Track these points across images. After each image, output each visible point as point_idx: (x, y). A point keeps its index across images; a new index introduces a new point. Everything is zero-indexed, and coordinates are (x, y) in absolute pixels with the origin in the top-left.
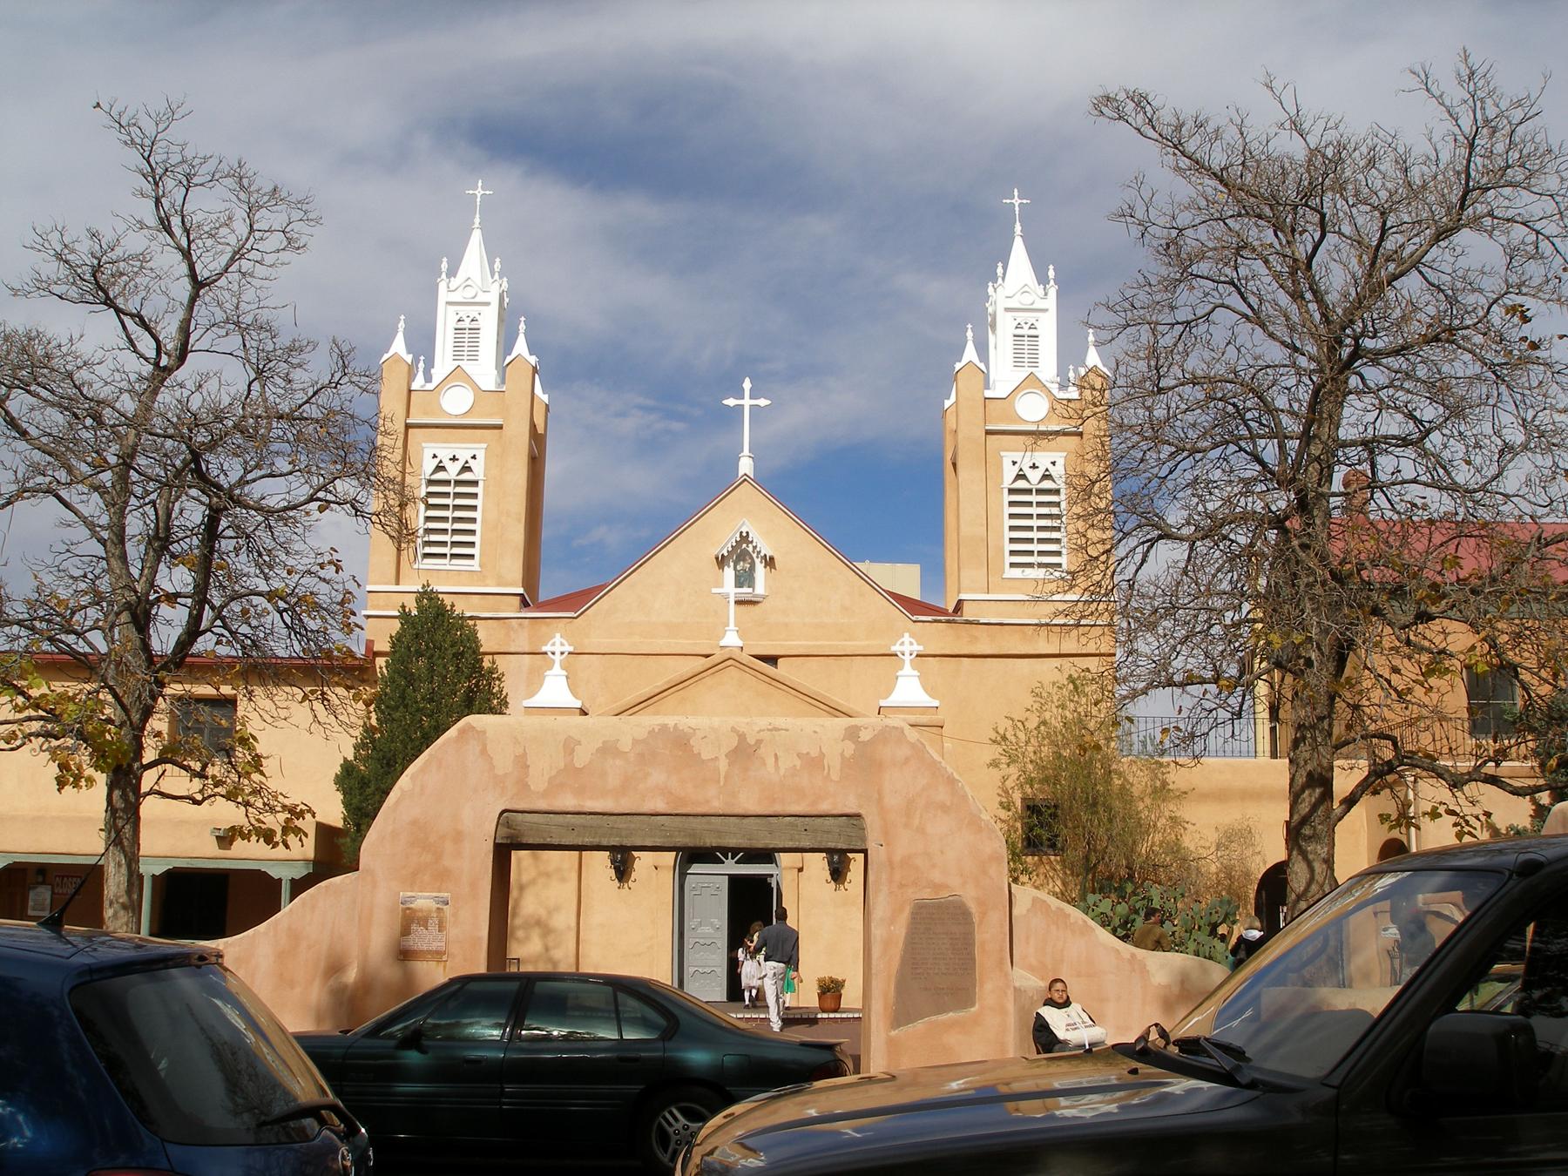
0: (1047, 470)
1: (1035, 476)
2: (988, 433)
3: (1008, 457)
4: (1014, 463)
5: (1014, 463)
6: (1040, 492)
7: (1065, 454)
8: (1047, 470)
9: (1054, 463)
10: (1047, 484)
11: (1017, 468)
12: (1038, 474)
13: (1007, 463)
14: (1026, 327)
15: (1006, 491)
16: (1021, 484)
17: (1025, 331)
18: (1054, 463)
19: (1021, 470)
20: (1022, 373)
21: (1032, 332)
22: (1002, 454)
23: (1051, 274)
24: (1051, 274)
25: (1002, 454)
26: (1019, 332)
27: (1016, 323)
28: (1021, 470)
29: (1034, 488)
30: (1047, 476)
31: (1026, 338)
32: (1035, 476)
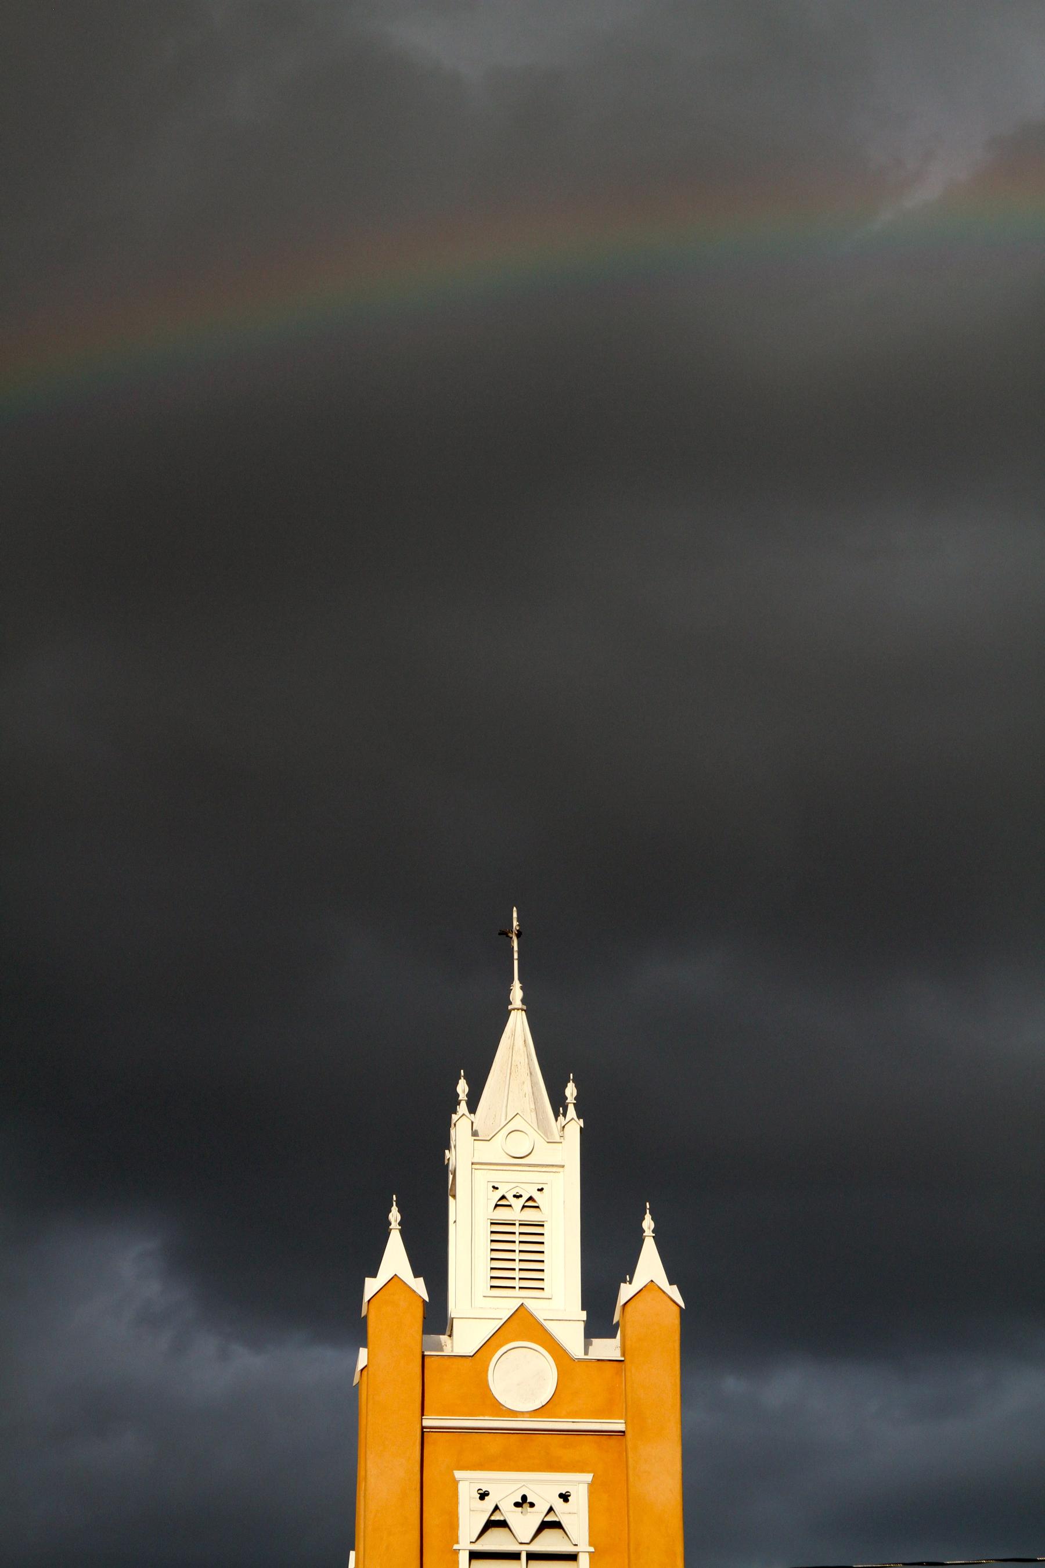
3: (468, 1482)
5: (483, 1496)
7: (588, 1477)
8: (551, 1509)
9: (565, 1497)
10: (550, 1542)
11: (489, 1504)
14: (518, 1204)
16: (496, 1541)
17: (515, 1213)
18: (565, 1497)
20: (505, 1306)
21: (530, 1215)
22: (458, 1474)
23: (571, 1091)
24: (571, 1091)
25: (458, 1474)
26: (503, 1214)
27: (498, 1194)
28: (496, 1508)
29: (524, 1549)
31: (517, 1229)
32: (524, 1524)
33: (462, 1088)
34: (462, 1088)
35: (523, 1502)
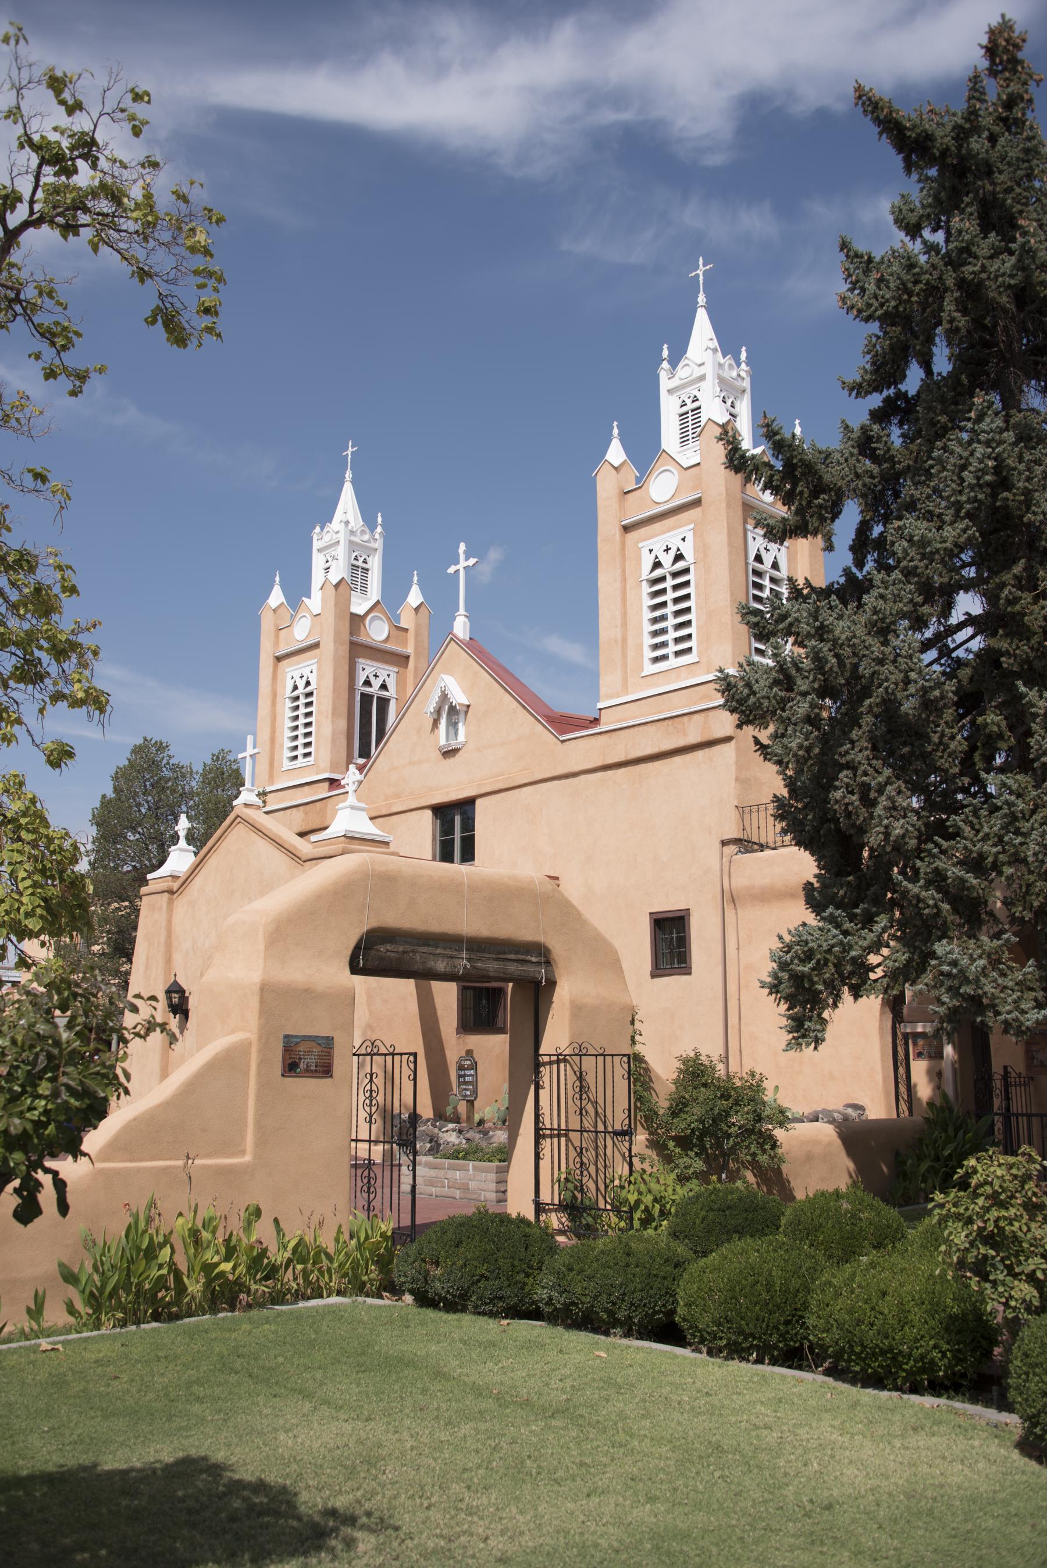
0: (678, 550)
1: (667, 560)
2: (626, 529)
3: (645, 546)
4: (651, 551)
5: (651, 551)
6: (675, 575)
7: (692, 526)
8: (678, 550)
9: (683, 539)
10: (680, 565)
12: (672, 553)
13: (645, 552)
15: (645, 584)
16: (658, 573)
18: (683, 539)
19: (657, 557)
21: (696, 405)
22: (640, 545)
26: (684, 409)
28: (657, 557)
30: (679, 557)
32: (667, 560)
33: (665, 353)
34: (665, 353)
35: (667, 550)
